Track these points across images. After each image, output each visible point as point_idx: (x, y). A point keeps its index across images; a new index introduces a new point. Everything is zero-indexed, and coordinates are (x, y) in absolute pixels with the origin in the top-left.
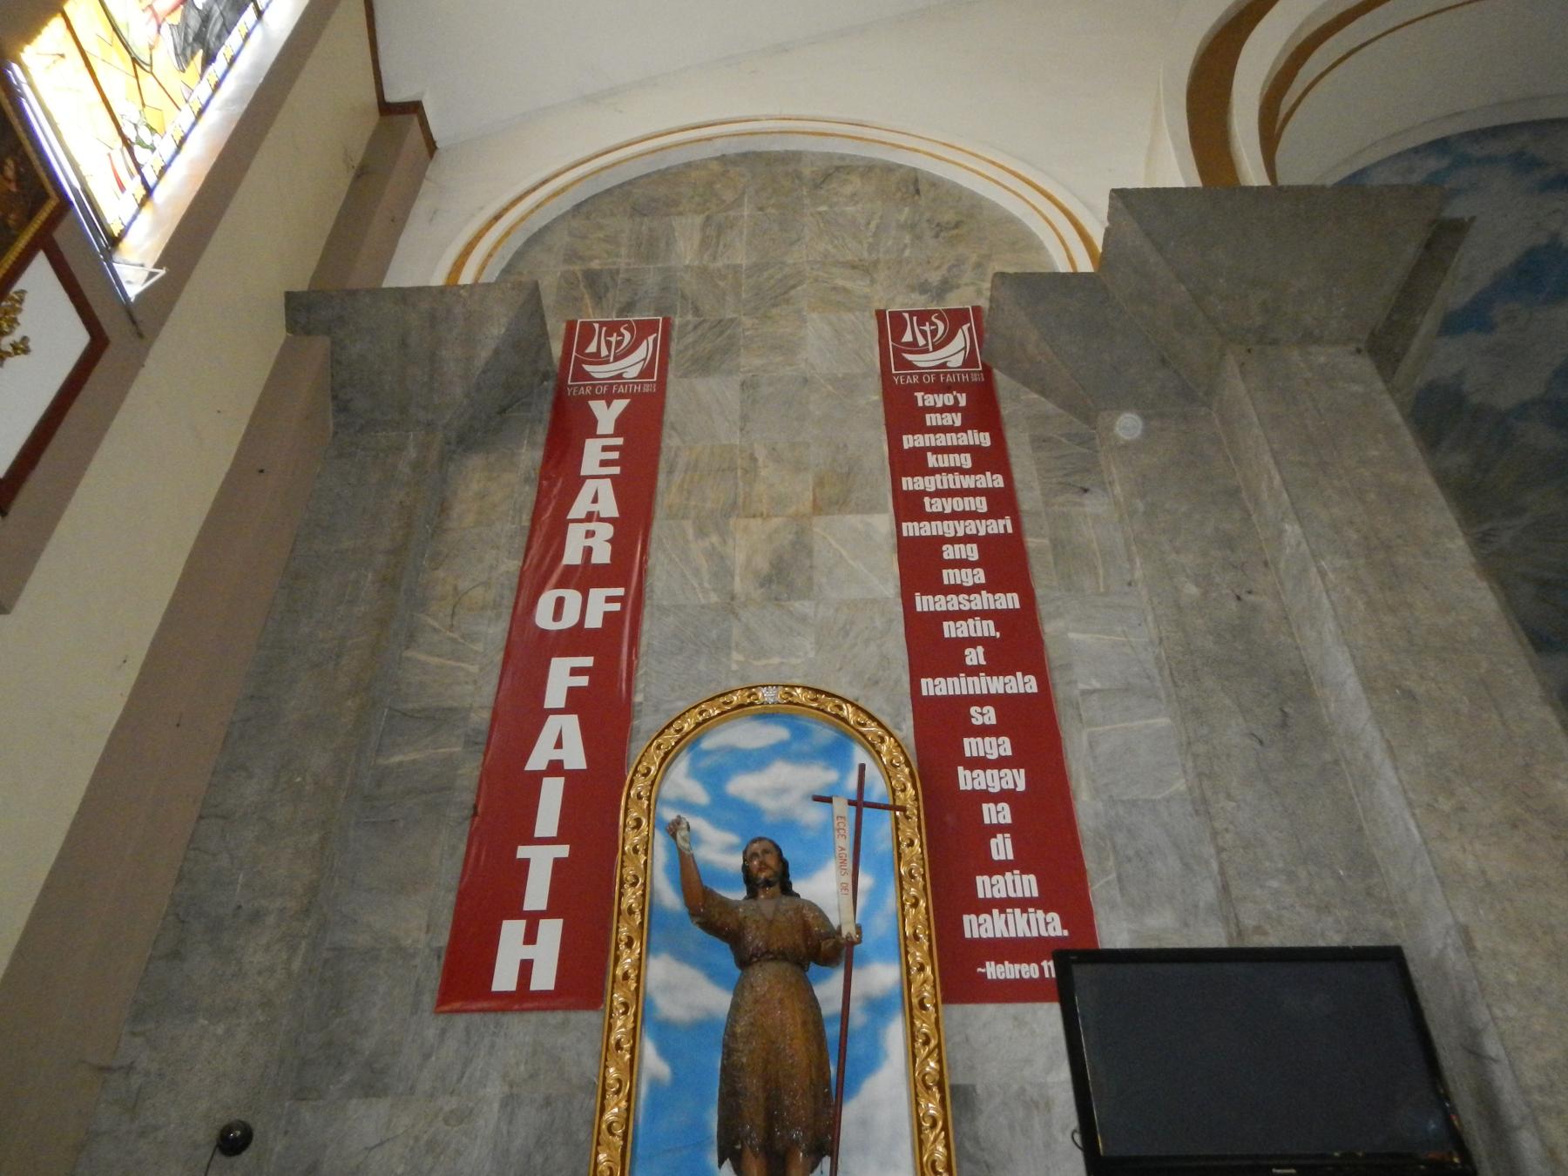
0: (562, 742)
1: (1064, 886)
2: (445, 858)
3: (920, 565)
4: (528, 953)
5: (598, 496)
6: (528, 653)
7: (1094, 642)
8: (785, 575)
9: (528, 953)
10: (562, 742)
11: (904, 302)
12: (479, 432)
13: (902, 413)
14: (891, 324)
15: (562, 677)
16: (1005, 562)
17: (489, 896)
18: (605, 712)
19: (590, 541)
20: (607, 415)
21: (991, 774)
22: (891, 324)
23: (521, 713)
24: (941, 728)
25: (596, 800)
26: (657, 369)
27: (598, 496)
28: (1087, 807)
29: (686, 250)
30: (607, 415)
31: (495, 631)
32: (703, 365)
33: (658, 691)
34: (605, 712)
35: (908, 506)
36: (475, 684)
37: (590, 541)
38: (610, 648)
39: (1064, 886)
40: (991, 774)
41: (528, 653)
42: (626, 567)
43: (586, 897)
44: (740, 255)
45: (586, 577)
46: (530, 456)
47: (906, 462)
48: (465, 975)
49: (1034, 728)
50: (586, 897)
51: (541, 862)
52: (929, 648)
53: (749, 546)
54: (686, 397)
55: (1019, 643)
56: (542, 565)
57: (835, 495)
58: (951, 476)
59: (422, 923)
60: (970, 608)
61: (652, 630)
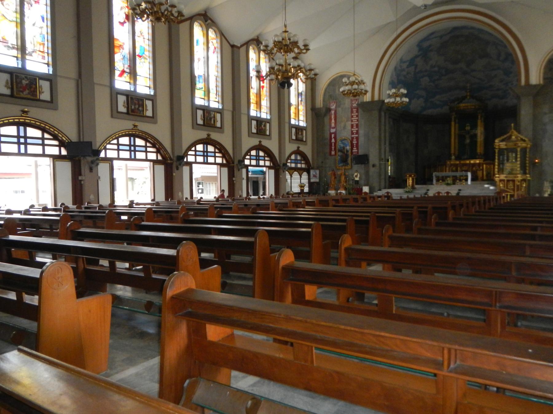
0: (333, 140)
2: (328, 147)
3: (352, 126)
4: (333, 153)
5: (333, 121)
7: (361, 132)
8: (345, 127)
9: (333, 153)
10: (333, 140)
12: (325, 115)
13: (352, 112)
15: (333, 136)
17: (331, 149)
18: (335, 138)
19: (333, 125)
21: (355, 142)
24: (353, 138)
26: (336, 107)
27: (333, 121)
28: (359, 144)
30: (333, 112)
34: (335, 138)
35: (352, 121)
36: (328, 136)
37: (333, 125)
41: (331, 134)
45: (333, 128)
48: (330, 154)
49: (357, 138)
51: (333, 148)
52: (352, 133)
53: (342, 125)
54: (339, 110)
55: (357, 133)
57: (347, 121)
58: (355, 118)
59: (328, 150)
61: (338, 132)
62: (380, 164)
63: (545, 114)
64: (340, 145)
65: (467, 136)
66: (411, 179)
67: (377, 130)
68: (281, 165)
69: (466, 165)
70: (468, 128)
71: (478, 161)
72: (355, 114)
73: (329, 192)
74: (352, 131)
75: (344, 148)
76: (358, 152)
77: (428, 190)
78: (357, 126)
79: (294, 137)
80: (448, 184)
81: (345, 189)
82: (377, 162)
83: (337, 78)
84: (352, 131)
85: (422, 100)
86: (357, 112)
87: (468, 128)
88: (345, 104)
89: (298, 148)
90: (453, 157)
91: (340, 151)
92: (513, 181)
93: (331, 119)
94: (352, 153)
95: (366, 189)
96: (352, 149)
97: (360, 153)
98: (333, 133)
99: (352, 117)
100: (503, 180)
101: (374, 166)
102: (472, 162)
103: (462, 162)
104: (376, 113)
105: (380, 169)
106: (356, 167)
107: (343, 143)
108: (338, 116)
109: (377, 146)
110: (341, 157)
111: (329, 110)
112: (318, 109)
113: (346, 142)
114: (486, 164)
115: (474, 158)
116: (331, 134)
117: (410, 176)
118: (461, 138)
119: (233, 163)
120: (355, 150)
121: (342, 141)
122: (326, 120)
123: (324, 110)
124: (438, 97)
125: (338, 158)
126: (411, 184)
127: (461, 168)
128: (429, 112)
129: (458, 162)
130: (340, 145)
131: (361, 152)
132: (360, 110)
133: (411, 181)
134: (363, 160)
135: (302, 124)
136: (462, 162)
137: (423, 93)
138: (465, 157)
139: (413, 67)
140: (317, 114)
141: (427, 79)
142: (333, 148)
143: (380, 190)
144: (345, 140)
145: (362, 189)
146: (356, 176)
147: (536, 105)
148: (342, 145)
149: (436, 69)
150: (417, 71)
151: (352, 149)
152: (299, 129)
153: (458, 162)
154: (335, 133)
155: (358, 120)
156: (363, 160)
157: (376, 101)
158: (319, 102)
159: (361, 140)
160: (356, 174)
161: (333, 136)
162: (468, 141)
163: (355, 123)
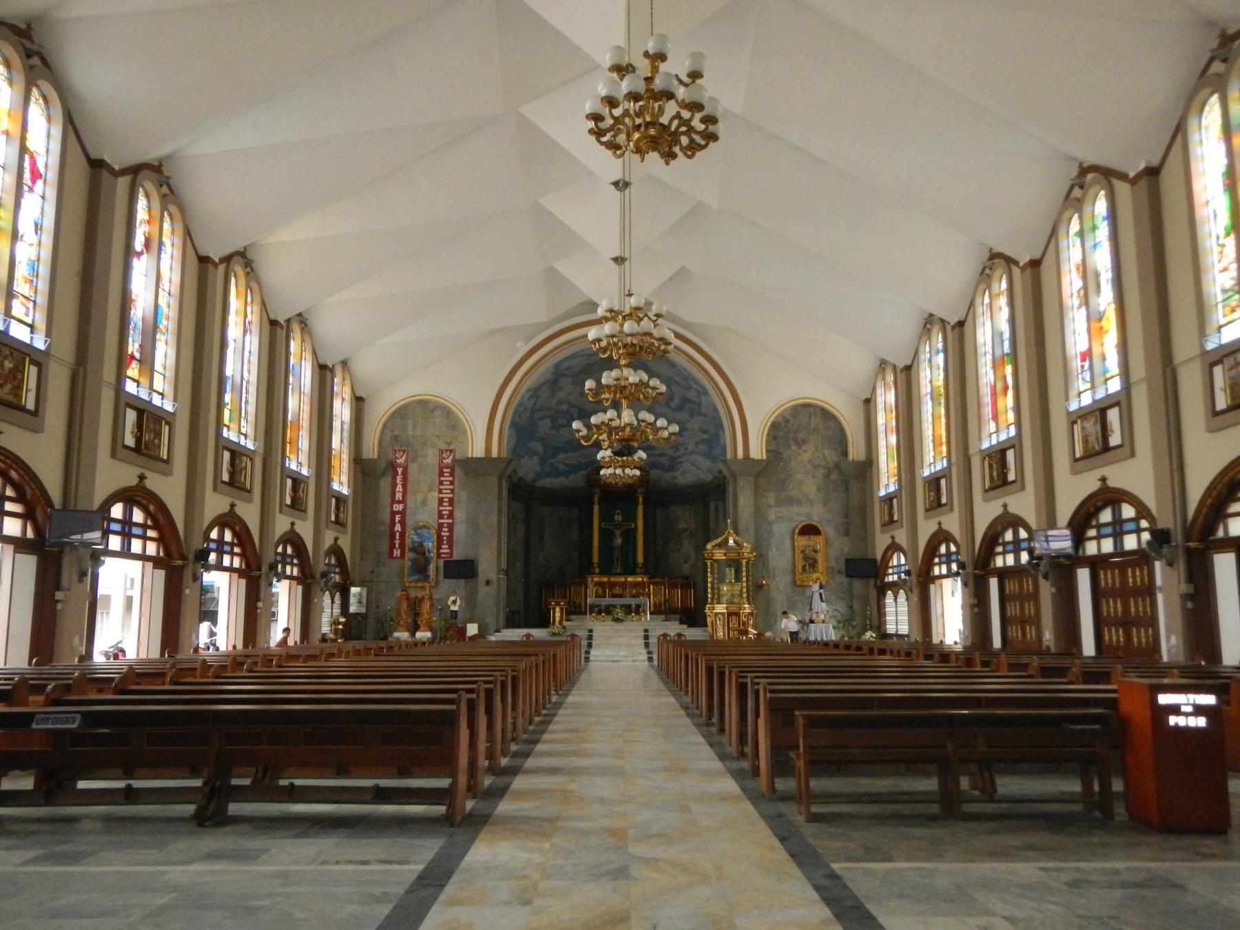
0: (398, 528)
1: (451, 547)
2: (387, 541)
3: (441, 501)
4: (397, 553)
5: (399, 488)
6: (393, 514)
7: (460, 515)
8: (424, 503)
9: (397, 553)
10: (398, 528)
11: (444, 447)
12: (384, 474)
13: (441, 474)
14: (442, 452)
16: (451, 502)
17: (392, 546)
18: (403, 523)
19: (399, 496)
20: (400, 470)
21: (445, 534)
22: (442, 452)
23: (393, 524)
24: (441, 526)
25: (403, 534)
26: (406, 460)
27: (399, 488)
29: (410, 432)
30: (400, 470)
31: (388, 510)
32: (413, 461)
33: (409, 522)
34: (403, 523)
35: (440, 491)
36: (387, 518)
38: (403, 513)
39: (451, 547)
40: (445, 534)
42: (403, 501)
43: (402, 546)
44: (419, 433)
45: (399, 502)
46: (390, 479)
47: (441, 483)
48: (391, 555)
49: (451, 526)
50: (402, 546)
51: (397, 542)
52: (441, 516)
53: (419, 497)
54: (413, 468)
55: (451, 515)
56: (393, 501)
57: (430, 490)
58: (447, 487)
59: (384, 548)
60: (446, 509)
62: (499, 579)
63: (770, 507)
64: (411, 537)
65: (618, 532)
66: (558, 609)
67: (496, 513)
68: (318, 576)
69: (623, 585)
70: (619, 518)
71: (640, 579)
72: (447, 478)
73: (396, 634)
74: (440, 512)
75: (421, 544)
76: (451, 554)
77: (591, 631)
78: (451, 502)
79: (333, 518)
80: (617, 620)
81: (431, 629)
82: (493, 576)
83: (410, 403)
84: (440, 512)
85: (536, 459)
86: (452, 474)
87: (619, 518)
88: (425, 456)
89: (336, 539)
90: (597, 570)
91: (413, 550)
92: (738, 614)
93: (394, 485)
94: (439, 555)
95: (472, 629)
96: (439, 547)
97: (456, 557)
98: (398, 513)
99: (441, 483)
100: (723, 614)
101: (488, 583)
102: (630, 579)
103: (613, 579)
104: (493, 481)
105: (499, 589)
106: (446, 584)
107: (418, 534)
108: (410, 478)
109: (495, 544)
110: (414, 561)
111: (393, 466)
112: (370, 460)
113: (424, 532)
114: (654, 584)
115: (633, 573)
116: (393, 514)
117: (558, 604)
118: (607, 535)
119: (259, 569)
120: (445, 549)
121: (416, 529)
122: (385, 484)
123: (384, 465)
124: (561, 456)
125: (407, 564)
126: (557, 619)
127: (611, 590)
128: (546, 482)
129: (605, 579)
130: (411, 537)
131: (457, 555)
132: (458, 471)
133: (558, 614)
134: (463, 570)
135: (345, 491)
136: (613, 579)
137: (539, 447)
138: (619, 570)
139: (533, 401)
140: (362, 468)
141: (548, 422)
142: (397, 542)
143: (498, 631)
144: (424, 527)
145: (464, 630)
146: (454, 602)
147: (758, 492)
148: (416, 539)
149: (564, 407)
150: (538, 406)
151: (439, 547)
152: (340, 499)
153: (605, 579)
154: (403, 513)
155: (452, 491)
156: (463, 570)
157: (495, 459)
158: (371, 449)
159: (460, 530)
160: (452, 598)
161: (398, 518)
162: (619, 541)
163: (447, 496)
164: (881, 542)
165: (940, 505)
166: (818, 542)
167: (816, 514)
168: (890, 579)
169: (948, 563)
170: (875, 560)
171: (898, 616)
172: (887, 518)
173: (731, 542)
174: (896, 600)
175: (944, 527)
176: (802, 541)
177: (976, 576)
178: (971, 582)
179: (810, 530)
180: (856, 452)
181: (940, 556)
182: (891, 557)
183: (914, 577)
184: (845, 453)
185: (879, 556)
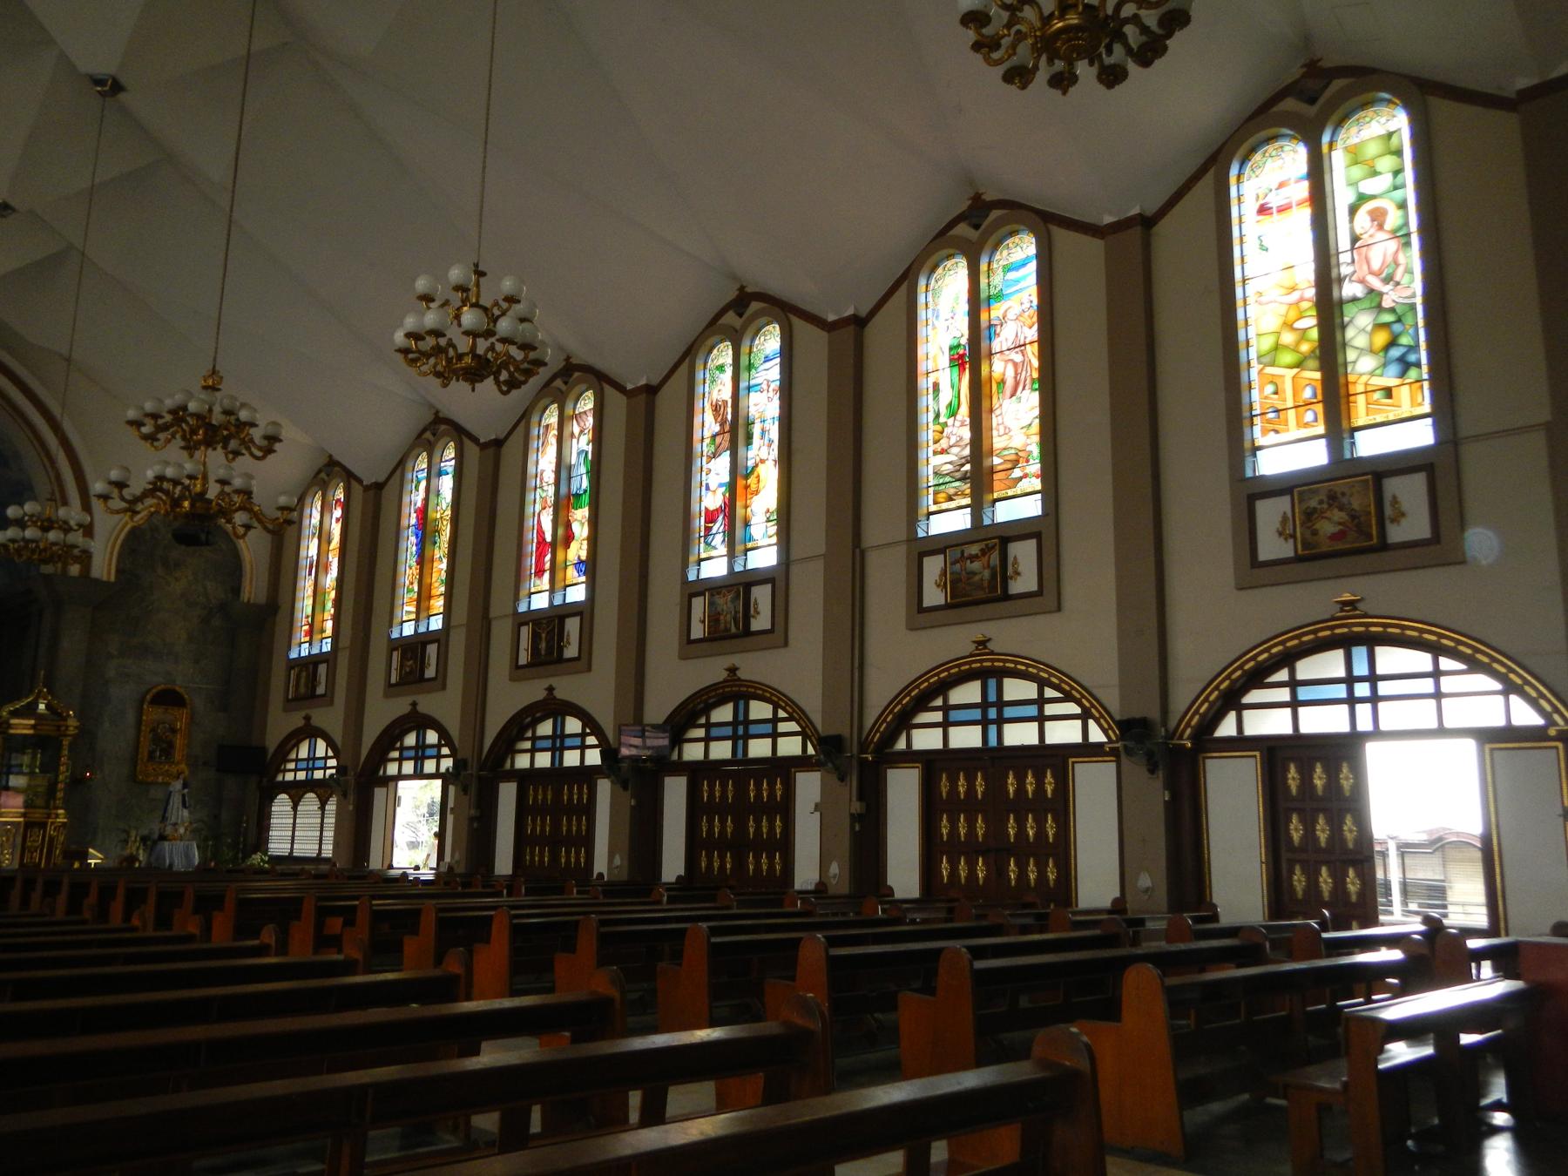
92: (43, 825)
164: (279, 723)
165: (422, 679)
166: (180, 719)
167: (183, 675)
168: (289, 777)
169: (419, 760)
170: (264, 750)
171: (300, 831)
172: (302, 690)
173: (42, 706)
174: (295, 808)
175: (420, 708)
176: (153, 714)
177: (480, 778)
178: (473, 789)
179: (169, 698)
180: (254, 589)
181: (402, 749)
182: (297, 745)
183: (351, 777)
184: (237, 591)
185: (272, 743)
